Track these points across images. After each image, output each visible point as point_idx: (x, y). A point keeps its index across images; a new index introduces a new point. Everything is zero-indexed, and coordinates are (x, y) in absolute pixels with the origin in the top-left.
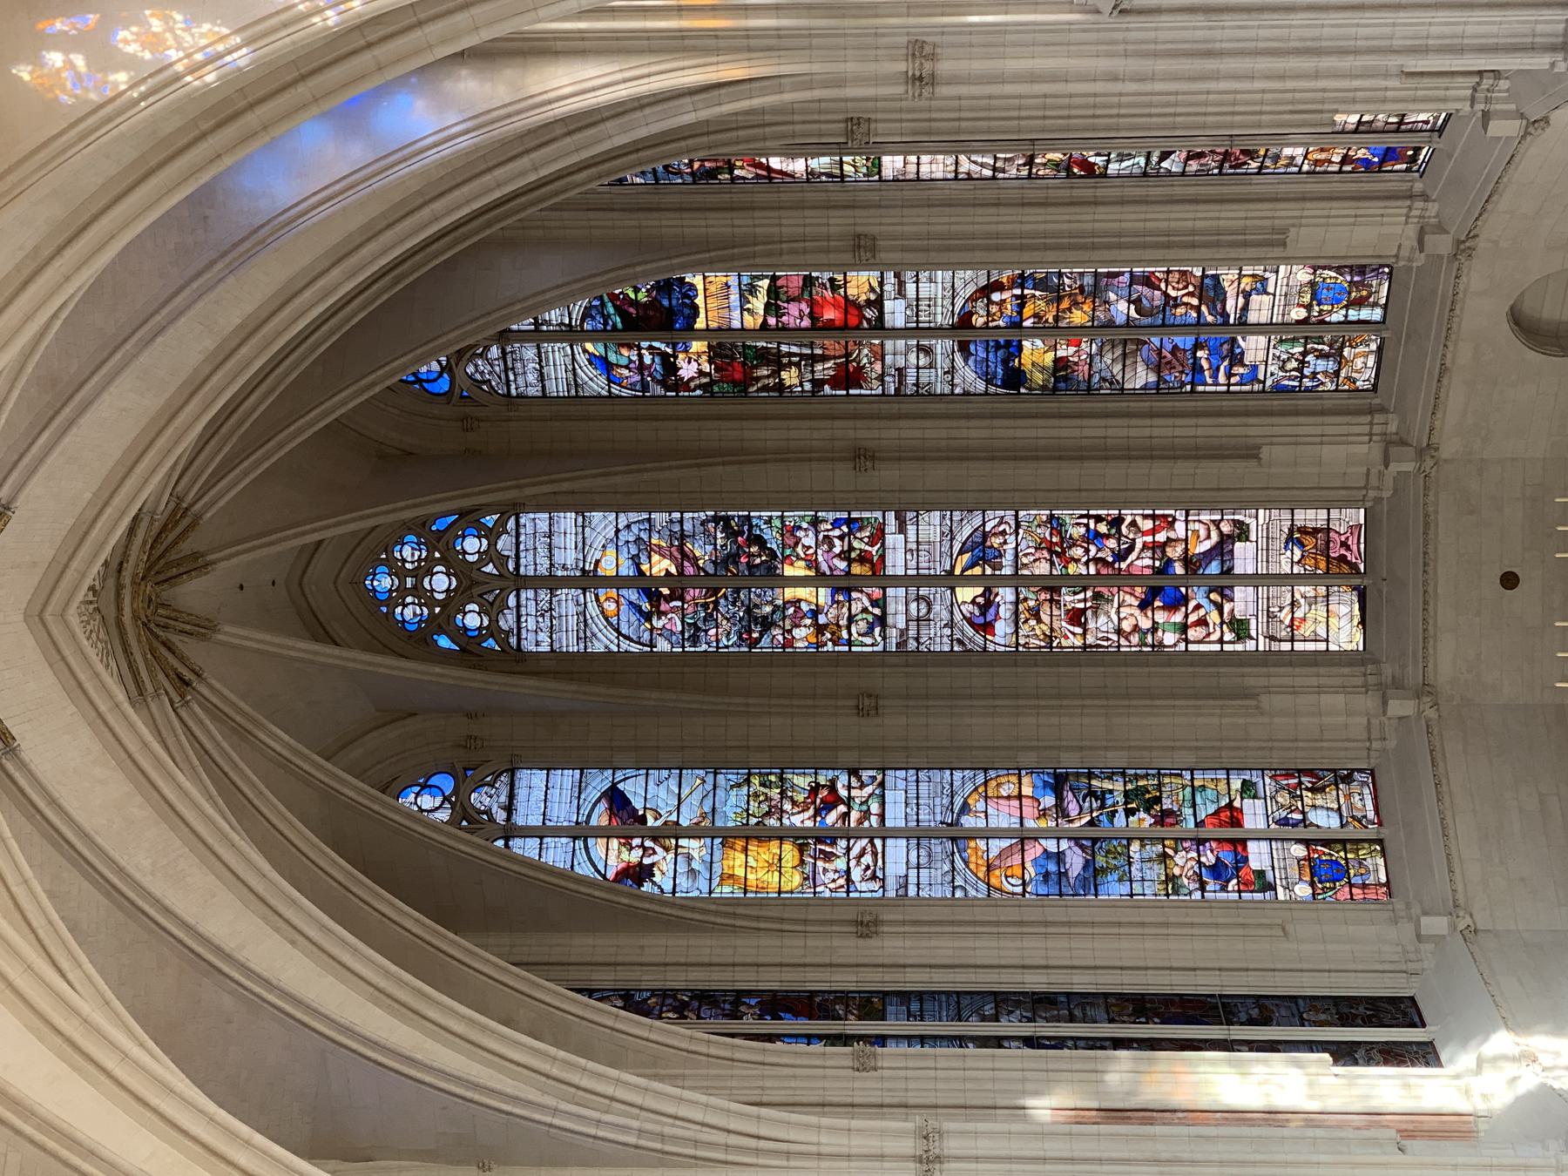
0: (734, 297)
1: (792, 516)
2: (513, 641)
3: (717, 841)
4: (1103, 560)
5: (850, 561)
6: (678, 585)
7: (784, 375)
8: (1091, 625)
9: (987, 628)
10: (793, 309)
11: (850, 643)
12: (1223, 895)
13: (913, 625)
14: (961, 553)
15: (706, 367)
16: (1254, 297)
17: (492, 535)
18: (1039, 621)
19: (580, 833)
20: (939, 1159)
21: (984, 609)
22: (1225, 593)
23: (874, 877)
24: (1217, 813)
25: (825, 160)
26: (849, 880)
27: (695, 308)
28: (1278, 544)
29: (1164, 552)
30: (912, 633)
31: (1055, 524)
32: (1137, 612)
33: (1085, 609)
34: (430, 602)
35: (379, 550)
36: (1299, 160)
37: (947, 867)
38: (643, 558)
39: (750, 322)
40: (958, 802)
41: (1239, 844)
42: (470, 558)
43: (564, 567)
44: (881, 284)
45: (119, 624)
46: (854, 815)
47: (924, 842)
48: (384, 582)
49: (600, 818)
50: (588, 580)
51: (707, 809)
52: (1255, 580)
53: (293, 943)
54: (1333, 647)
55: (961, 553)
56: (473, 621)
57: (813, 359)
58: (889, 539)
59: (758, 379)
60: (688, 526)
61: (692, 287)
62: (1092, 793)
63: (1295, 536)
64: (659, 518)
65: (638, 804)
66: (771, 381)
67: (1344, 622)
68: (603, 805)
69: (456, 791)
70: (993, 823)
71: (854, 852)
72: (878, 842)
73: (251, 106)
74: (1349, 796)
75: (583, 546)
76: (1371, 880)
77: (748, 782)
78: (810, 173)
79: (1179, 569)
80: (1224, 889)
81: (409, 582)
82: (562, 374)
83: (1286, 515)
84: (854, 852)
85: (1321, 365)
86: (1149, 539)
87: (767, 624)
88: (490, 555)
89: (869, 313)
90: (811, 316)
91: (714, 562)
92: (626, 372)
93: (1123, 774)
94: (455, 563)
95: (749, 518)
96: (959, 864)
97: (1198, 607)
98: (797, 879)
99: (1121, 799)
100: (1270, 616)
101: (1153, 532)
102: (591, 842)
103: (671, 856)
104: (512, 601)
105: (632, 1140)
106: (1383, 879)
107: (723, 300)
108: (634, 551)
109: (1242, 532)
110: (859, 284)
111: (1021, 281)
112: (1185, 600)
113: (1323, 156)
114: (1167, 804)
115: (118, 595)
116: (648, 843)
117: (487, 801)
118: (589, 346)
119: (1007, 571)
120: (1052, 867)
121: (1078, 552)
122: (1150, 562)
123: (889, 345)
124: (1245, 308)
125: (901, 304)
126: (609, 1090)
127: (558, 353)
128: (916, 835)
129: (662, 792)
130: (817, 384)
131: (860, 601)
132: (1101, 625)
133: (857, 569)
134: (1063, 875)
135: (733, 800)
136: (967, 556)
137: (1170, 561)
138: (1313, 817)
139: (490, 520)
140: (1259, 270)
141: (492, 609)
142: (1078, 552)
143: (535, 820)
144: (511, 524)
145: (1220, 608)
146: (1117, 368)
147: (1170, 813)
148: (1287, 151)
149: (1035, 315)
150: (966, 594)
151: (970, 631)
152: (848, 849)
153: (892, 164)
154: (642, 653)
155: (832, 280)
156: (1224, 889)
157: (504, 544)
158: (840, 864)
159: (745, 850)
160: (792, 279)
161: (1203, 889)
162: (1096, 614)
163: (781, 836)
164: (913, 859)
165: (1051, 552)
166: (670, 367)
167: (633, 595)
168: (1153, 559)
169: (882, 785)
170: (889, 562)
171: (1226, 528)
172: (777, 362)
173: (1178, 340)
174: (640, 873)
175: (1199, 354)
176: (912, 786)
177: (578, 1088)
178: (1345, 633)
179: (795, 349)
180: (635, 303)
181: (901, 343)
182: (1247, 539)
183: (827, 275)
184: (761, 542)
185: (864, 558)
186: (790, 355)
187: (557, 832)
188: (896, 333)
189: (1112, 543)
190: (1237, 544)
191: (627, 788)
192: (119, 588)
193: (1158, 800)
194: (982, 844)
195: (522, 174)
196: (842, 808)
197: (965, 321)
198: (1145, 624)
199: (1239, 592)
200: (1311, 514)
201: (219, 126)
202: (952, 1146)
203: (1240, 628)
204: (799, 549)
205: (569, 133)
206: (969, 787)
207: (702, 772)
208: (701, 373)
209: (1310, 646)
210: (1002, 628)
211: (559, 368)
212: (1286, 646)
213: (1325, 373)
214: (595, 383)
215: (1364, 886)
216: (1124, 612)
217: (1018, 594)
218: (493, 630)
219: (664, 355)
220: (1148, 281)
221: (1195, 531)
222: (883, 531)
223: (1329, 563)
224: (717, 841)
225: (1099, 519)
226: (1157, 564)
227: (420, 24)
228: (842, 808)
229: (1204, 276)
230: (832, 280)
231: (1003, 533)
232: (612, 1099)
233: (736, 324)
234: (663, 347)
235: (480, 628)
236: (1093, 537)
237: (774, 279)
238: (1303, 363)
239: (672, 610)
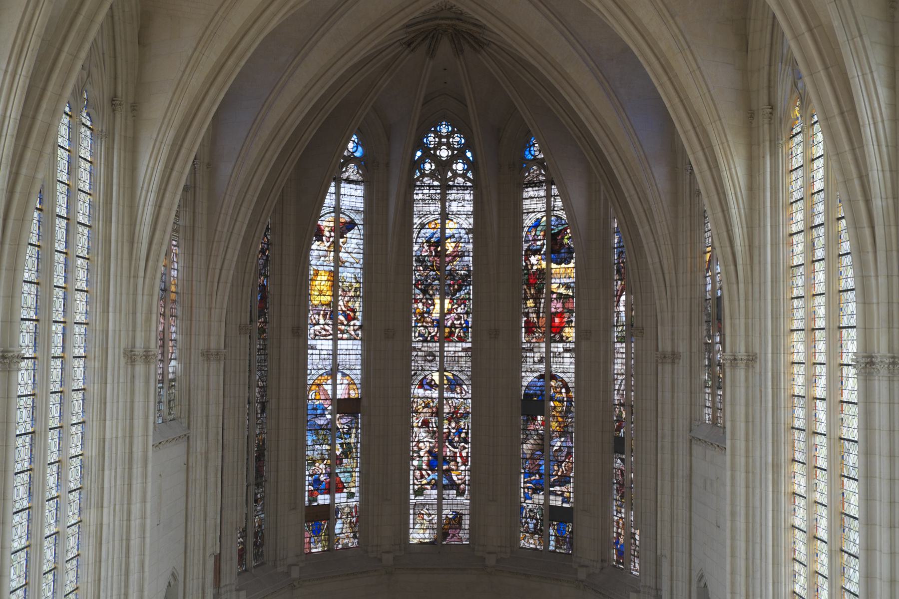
0: (564, 281)
1: (470, 304)
2: (418, 183)
3: (332, 269)
4: (449, 435)
5: (450, 327)
6: (441, 255)
7: (531, 301)
8: (422, 430)
9: (421, 386)
10: (559, 305)
11: (416, 326)
12: (307, 483)
13: (423, 354)
14: (453, 375)
15: (535, 267)
16: (561, 498)
17: (464, 176)
18: (424, 408)
19: (337, 210)
20: (208, 360)
21: (429, 384)
22: (435, 485)
23: (316, 335)
24: (343, 483)
25: (624, 319)
26: (314, 325)
27: (560, 264)
28: (455, 508)
30: (420, 353)
31: (465, 416)
32: (427, 449)
33: (428, 427)
34: (435, 149)
35: (459, 126)
36: (619, 515)
37: (320, 367)
38: (453, 240)
39: (554, 286)
40: (347, 372)
41: (327, 491)
42: (454, 166)
43: (450, 206)
44: (570, 342)
45: (436, 18)
46: (343, 327)
47: (331, 357)
48: (444, 130)
49: (343, 219)
50: (445, 216)
51: (346, 264)
52: (440, 498)
53: (305, 87)
54: (411, 531)
55: (453, 375)
56: (427, 166)
57: (538, 313)
58: (459, 344)
59: (530, 289)
60: (466, 258)
61: (569, 263)
62: (350, 429)
63: (458, 517)
64: (471, 246)
65: (349, 235)
66: (529, 295)
67: (422, 536)
68: (348, 219)
69: (355, 157)
70: (339, 387)
71: (327, 327)
72: (331, 337)
73: (670, 79)
74: (348, 537)
75: (458, 214)
76: (312, 546)
77: (357, 282)
78: (619, 313)
79: (445, 467)
80: (310, 484)
81: (444, 140)
82: (533, 206)
83: (467, 512)
84: (327, 327)
85: (531, 526)
87: (424, 292)
88: (455, 175)
89: (557, 336)
90: (557, 312)
91: (450, 270)
92: (533, 234)
93: (357, 442)
94: (452, 159)
95: (469, 285)
96: (321, 372)
97: (429, 475)
98: (316, 303)
99: (347, 441)
100: (425, 505)
101: (461, 456)
102: (333, 215)
103: (326, 248)
104: (436, 183)
105: (219, 228)
106: (313, 551)
107: (563, 274)
108: (456, 236)
109: (460, 493)
110: (570, 333)
111: (570, 400)
112: (432, 470)
113: (621, 525)
114: (345, 461)
115: (448, 18)
116: (332, 239)
117: (351, 170)
118: (544, 219)
119: (446, 395)
120: (319, 412)
121: (453, 425)
122: (448, 454)
123: (543, 345)
124: (556, 495)
125: (561, 350)
126: (240, 219)
127: (541, 206)
128: (335, 353)
129: (353, 246)
130: (527, 315)
131: (434, 331)
132: (422, 434)
133: (447, 330)
134: (316, 416)
135: (349, 275)
136: (451, 377)
137: (448, 463)
138: (339, 521)
139: (470, 175)
140: (572, 500)
141: (432, 175)
142: (453, 425)
143: (342, 191)
144: (469, 184)
145: (428, 484)
146: (532, 441)
147: (341, 463)
148: (623, 511)
149: (555, 407)
150: (436, 377)
151: (420, 378)
152: (328, 325)
153: (620, 347)
154: (412, 238)
155: (572, 321)
156: (310, 484)
157: (460, 180)
158: (322, 321)
159: (328, 280)
160: (572, 304)
161: (310, 475)
162: (425, 432)
163: (335, 296)
164: (323, 352)
165: (453, 413)
166: (536, 252)
167: (438, 235)
169: (355, 339)
170: (451, 344)
171: (462, 486)
172: (536, 300)
173: (543, 467)
174: (319, 235)
175: (537, 476)
176: (354, 352)
177: (241, 206)
178: (419, 535)
179: (542, 305)
180: (563, 238)
181: (544, 350)
182: (457, 496)
183: (574, 319)
184: (459, 290)
185: (452, 333)
186: (540, 303)
187: (338, 200)
188: (548, 348)
189: (457, 439)
190: (455, 492)
191: (355, 231)
192: (451, 19)
193: (347, 457)
194: (330, 382)
195: (628, 190)
196: (345, 323)
197: (554, 377)
198: (422, 453)
199: (435, 492)
200: (468, 522)
201: (662, 66)
202: (213, 365)
203: (419, 492)
204: (456, 306)
205: (645, 211)
206: (353, 377)
207: (361, 262)
208: (533, 265)
209: (411, 521)
210: (421, 392)
211: (534, 204)
212: (411, 512)
213: (528, 527)
214: (528, 221)
215: (310, 543)
216: (428, 444)
218: (423, 175)
219: (540, 250)
220: (569, 454)
221: (461, 474)
222: (462, 342)
223: (447, 528)
224: (332, 269)
225: (467, 433)
227: (703, 149)
228: (345, 323)
229: (570, 477)
230: (572, 321)
231: (461, 393)
232: (236, 220)
233: (553, 281)
234: (544, 249)
235: (424, 169)
236: (459, 431)
237: (572, 297)
238: (532, 518)
239: (431, 252)
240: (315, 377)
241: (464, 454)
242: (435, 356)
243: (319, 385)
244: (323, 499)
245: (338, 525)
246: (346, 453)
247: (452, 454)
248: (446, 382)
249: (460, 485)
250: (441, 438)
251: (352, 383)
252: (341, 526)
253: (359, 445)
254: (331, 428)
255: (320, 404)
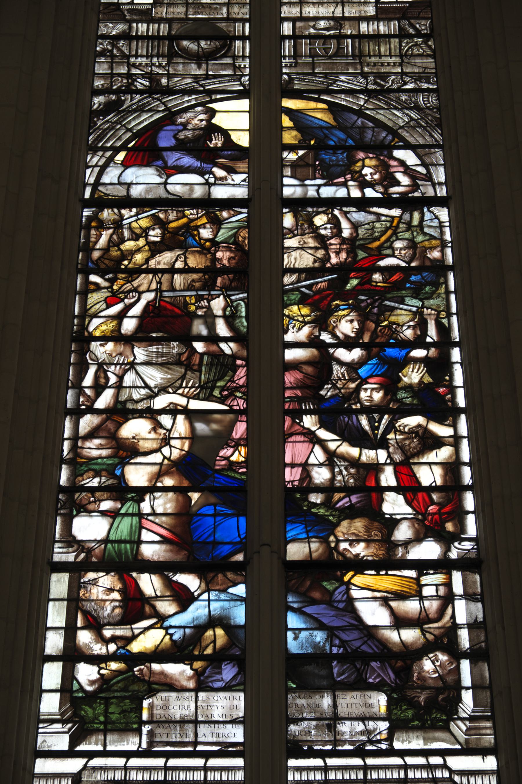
29: (350, 513)
30: (142, 28)
86: (388, 478)
122: (321, 475)
137: (321, 527)
150: (235, 118)
168: (328, 489)
189: (372, 394)
217: (230, 204)
226: (316, 498)
241: (428, 475)
242: (226, 40)
247: (345, 476)
248: (289, 137)
249: (412, 654)
250: (269, 395)
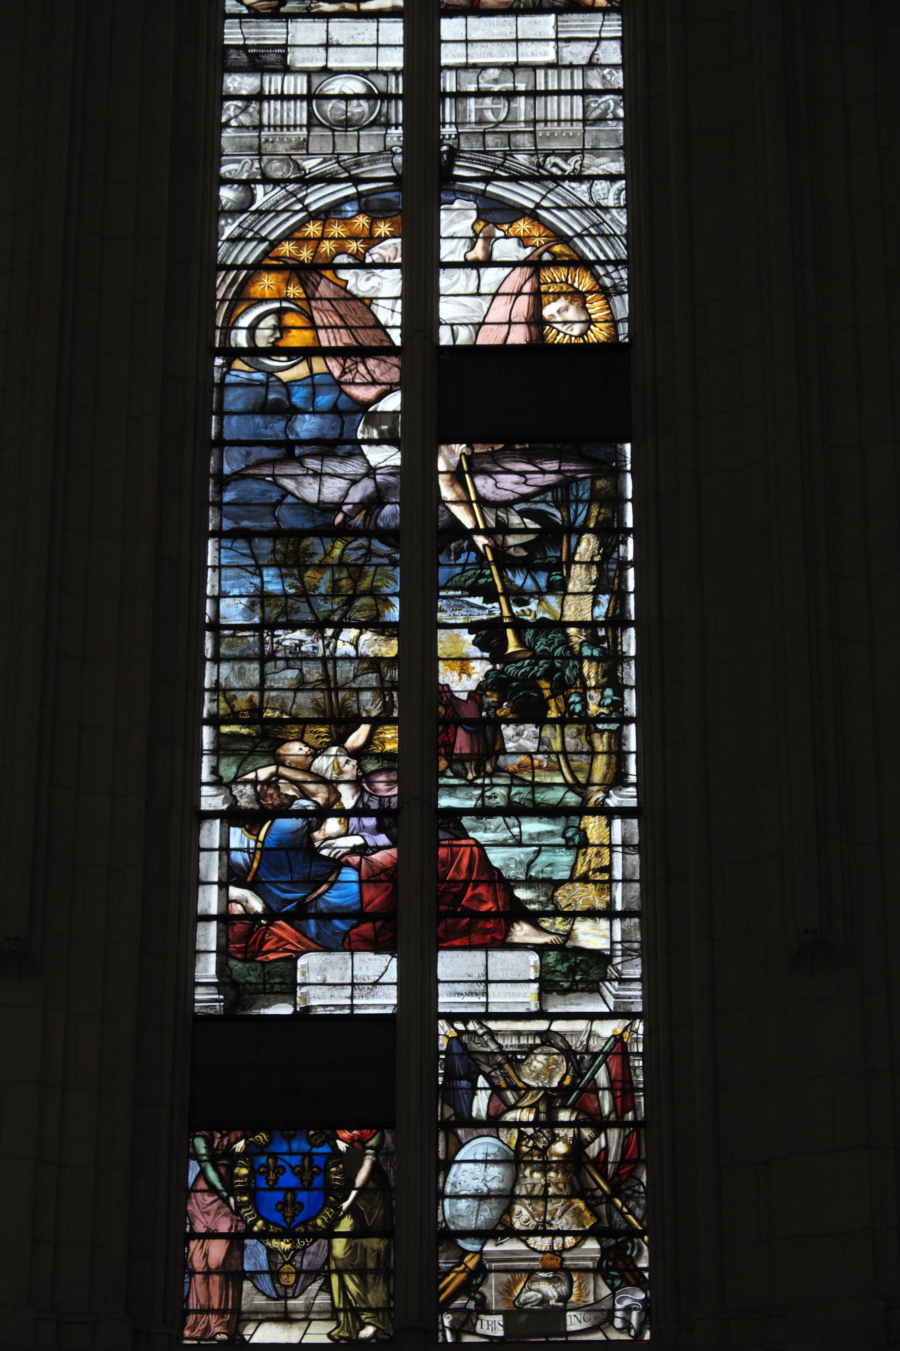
40: (525, 195)
80: (233, 875)
93: (617, 621)
96: (320, 197)
114: (518, 738)
194: (390, 249)
240: (274, 228)
243: (304, 273)
244: (350, 981)
245: (474, 1169)
246: (519, 694)
251: (554, 257)
252: (495, 1177)
253: (630, 643)
254: (417, 541)
255: (312, 383)
